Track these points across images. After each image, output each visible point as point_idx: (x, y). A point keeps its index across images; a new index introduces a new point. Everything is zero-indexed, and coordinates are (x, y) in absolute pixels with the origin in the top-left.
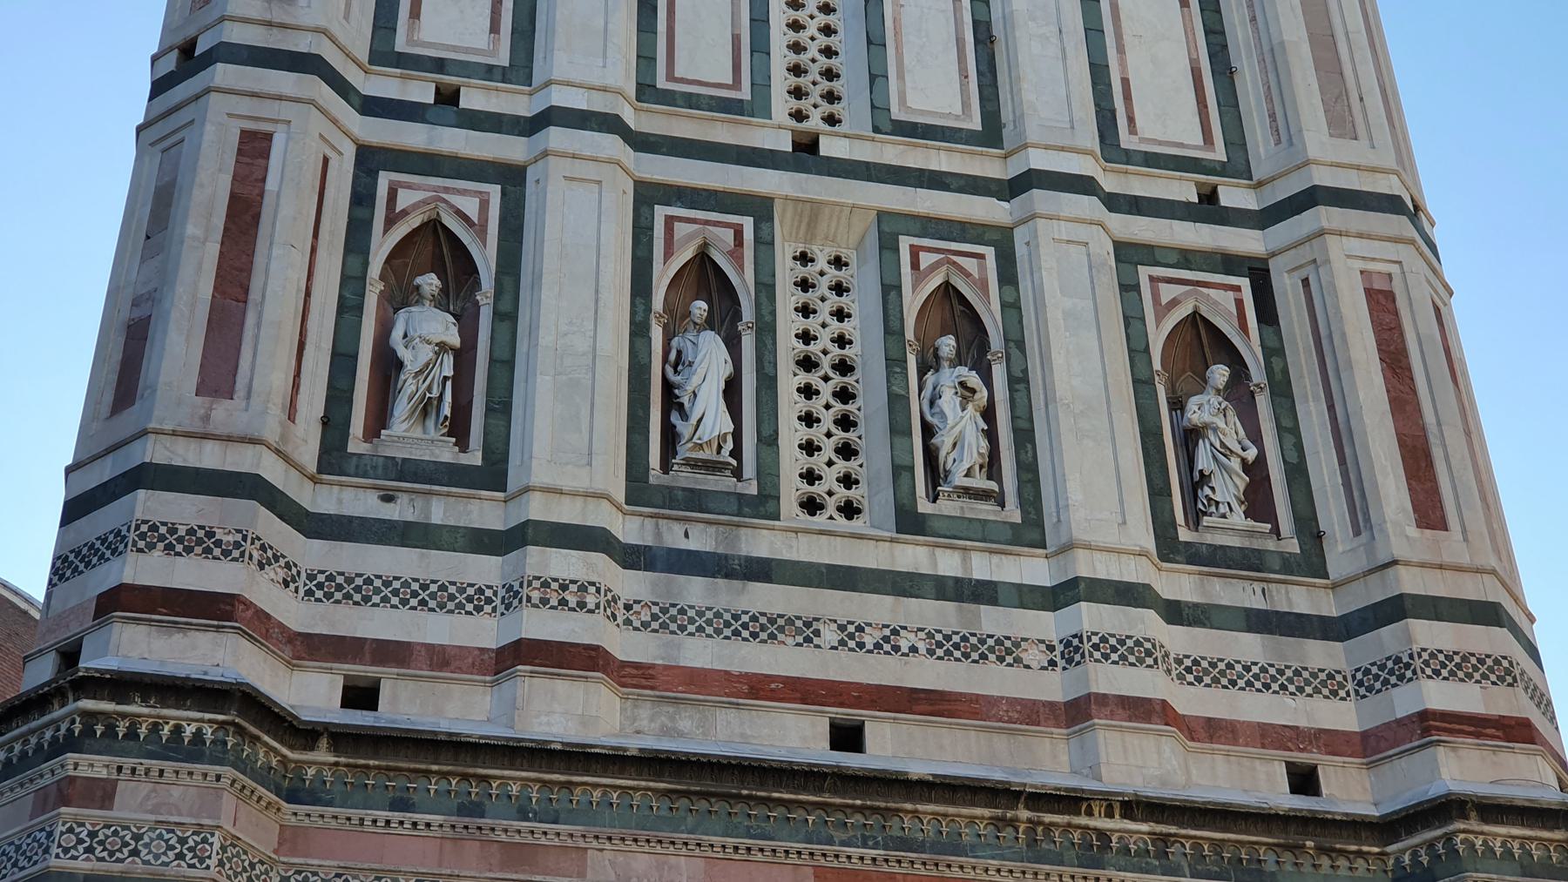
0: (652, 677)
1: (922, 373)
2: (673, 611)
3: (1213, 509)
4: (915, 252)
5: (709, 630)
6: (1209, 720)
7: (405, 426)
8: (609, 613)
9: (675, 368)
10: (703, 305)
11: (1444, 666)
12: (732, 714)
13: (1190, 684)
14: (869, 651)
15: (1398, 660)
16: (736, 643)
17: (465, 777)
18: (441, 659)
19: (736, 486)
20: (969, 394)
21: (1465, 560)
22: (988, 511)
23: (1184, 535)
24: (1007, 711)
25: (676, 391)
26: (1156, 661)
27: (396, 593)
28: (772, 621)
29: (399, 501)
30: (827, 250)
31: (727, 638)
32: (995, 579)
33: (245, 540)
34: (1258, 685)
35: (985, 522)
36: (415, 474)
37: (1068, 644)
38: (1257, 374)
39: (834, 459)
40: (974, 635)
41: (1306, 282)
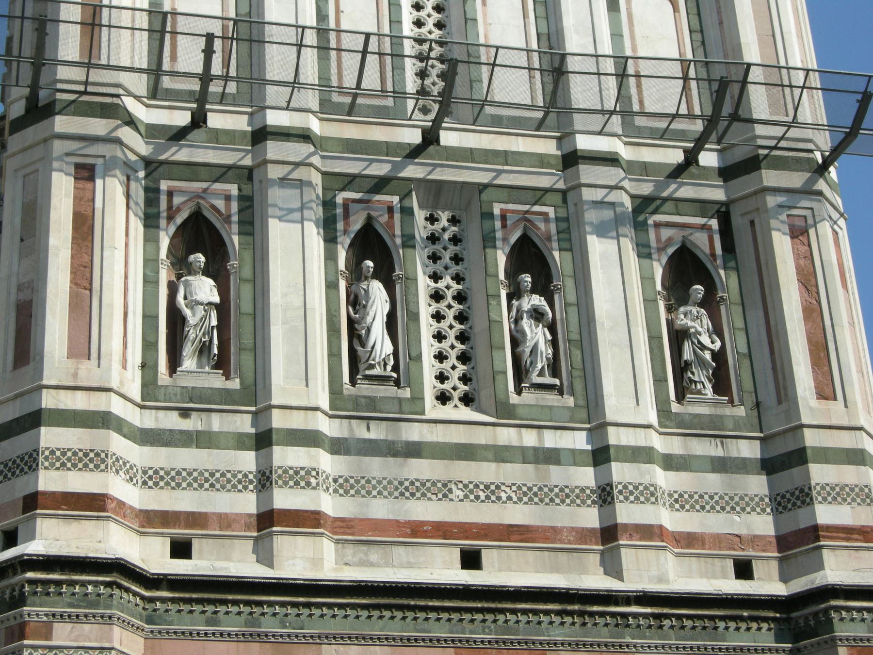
0: (352, 527)
1: (510, 297)
2: (363, 482)
5: (385, 493)
6: (689, 533)
8: (325, 487)
9: (354, 309)
10: (370, 263)
11: (829, 494)
12: (401, 550)
13: (678, 510)
14: (483, 501)
15: (802, 491)
16: (402, 501)
17: (247, 603)
18: (225, 521)
19: (397, 393)
20: (538, 316)
21: (845, 422)
23: (675, 407)
24: (567, 536)
25: (356, 325)
26: (657, 499)
27: (195, 480)
28: (423, 484)
29: (192, 417)
31: (396, 498)
32: (558, 446)
33: (107, 457)
34: (718, 508)
35: (551, 408)
36: (200, 397)
39: (457, 364)
40: (546, 486)
41: (752, 223)
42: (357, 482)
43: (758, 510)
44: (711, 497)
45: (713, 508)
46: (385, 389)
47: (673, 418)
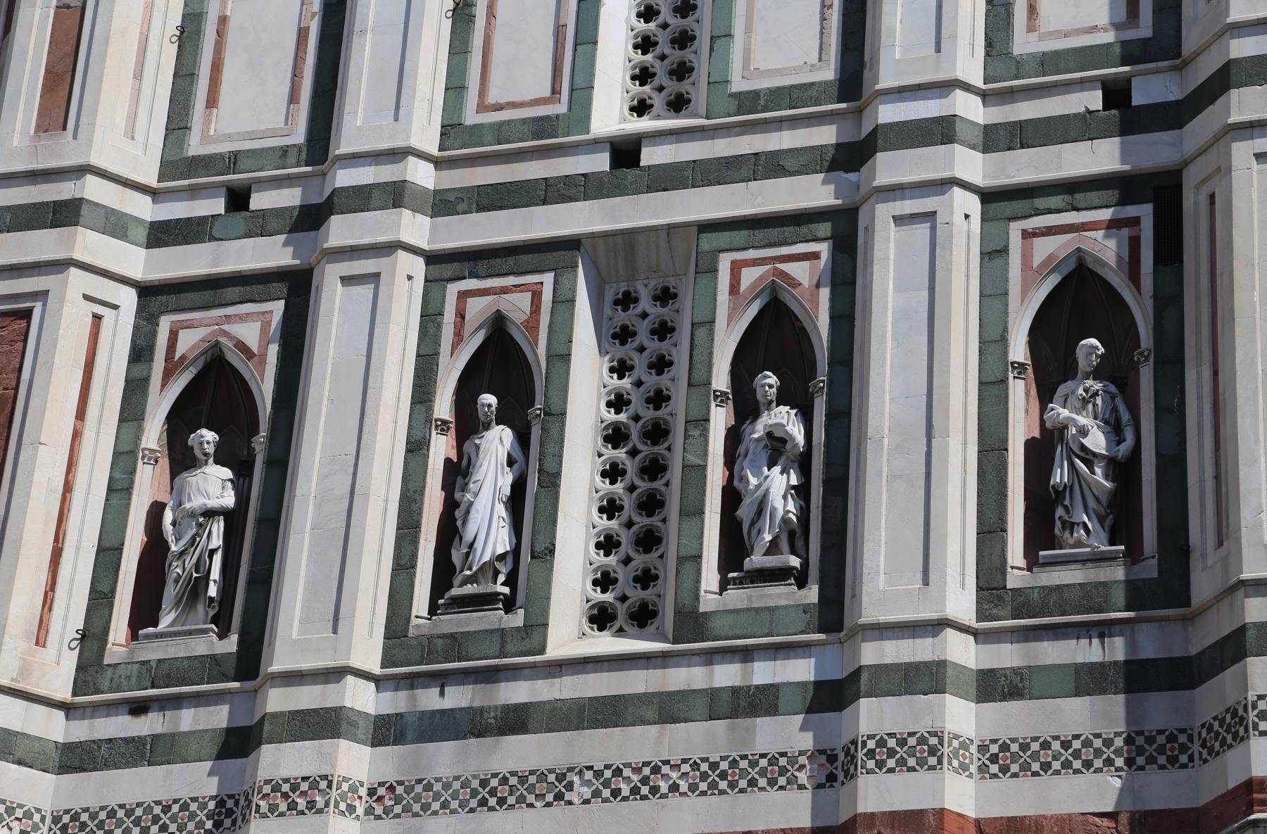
2: (419, 788)
3: (1067, 534)
4: (736, 268)
7: (172, 616)
13: (995, 776)
14: (625, 799)
16: (483, 814)
20: (778, 445)
22: (779, 595)
30: (653, 283)
32: (778, 680)
34: (1077, 764)
35: (771, 610)
37: (847, 753)
38: (1146, 339)
39: (632, 554)
41: (1212, 197)
42: (409, 790)
43: (1162, 760)
44: (1066, 745)
45: (1067, 765)
46: (480, 618)
47: (1008, 598)
